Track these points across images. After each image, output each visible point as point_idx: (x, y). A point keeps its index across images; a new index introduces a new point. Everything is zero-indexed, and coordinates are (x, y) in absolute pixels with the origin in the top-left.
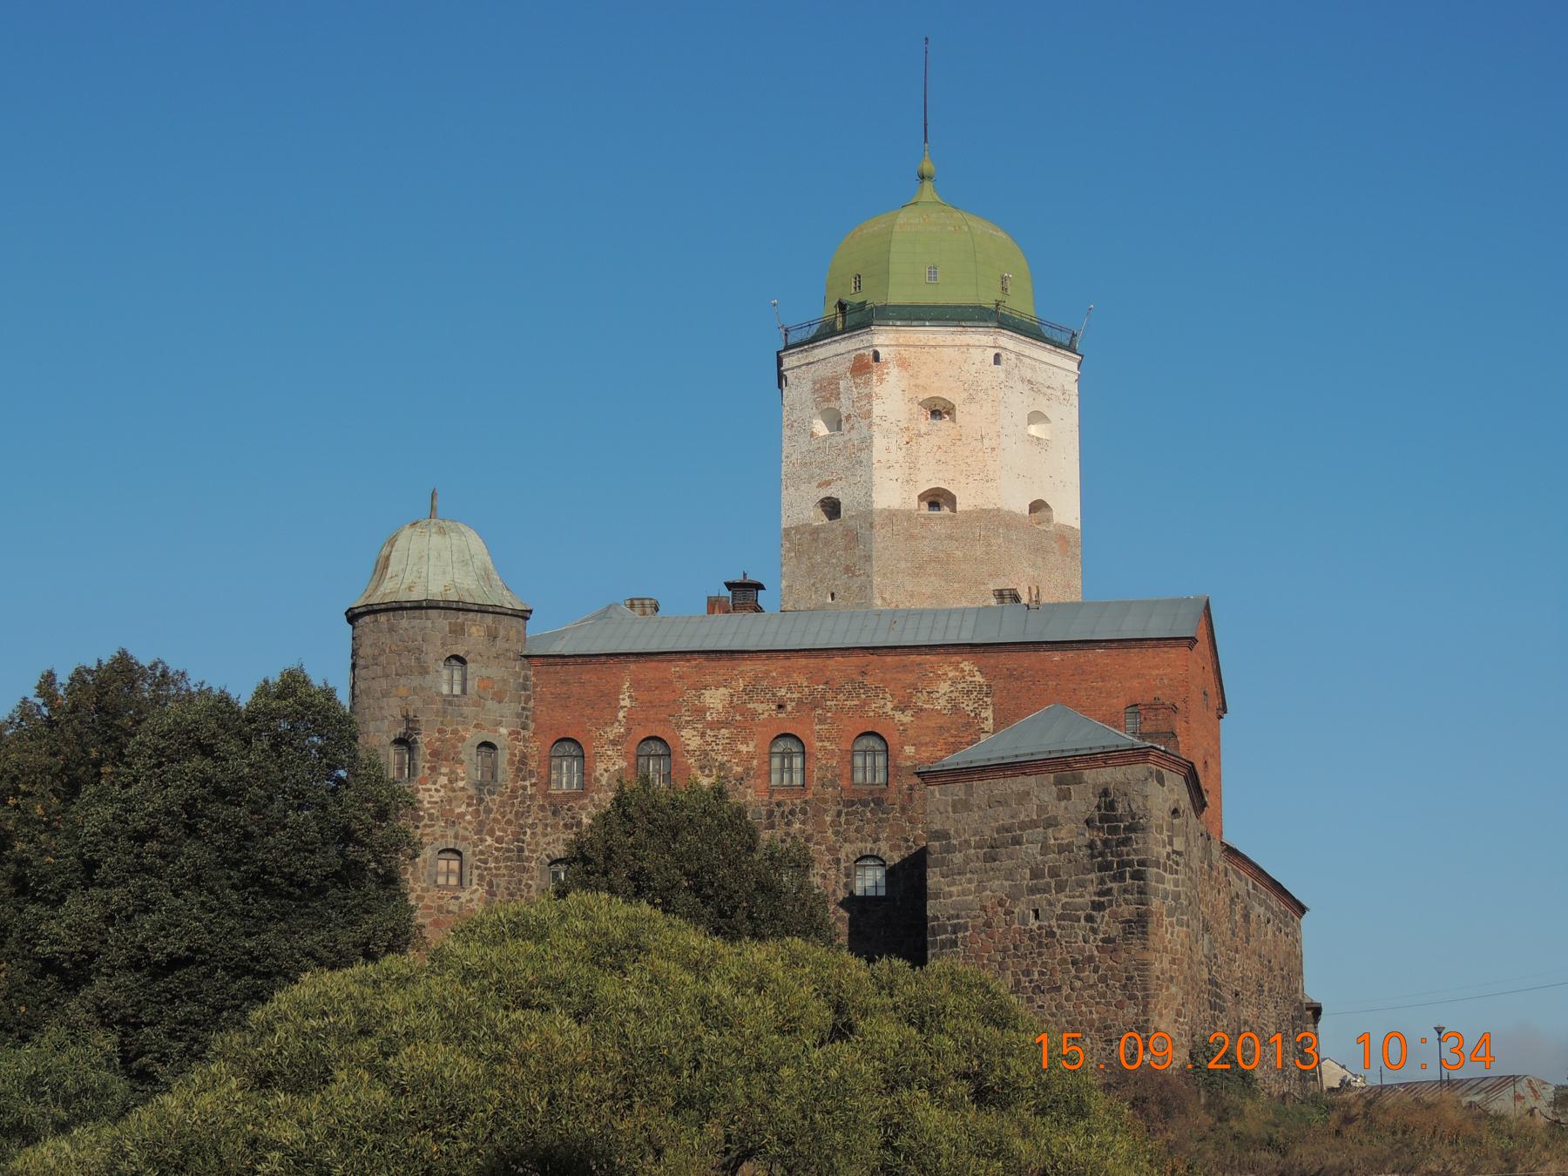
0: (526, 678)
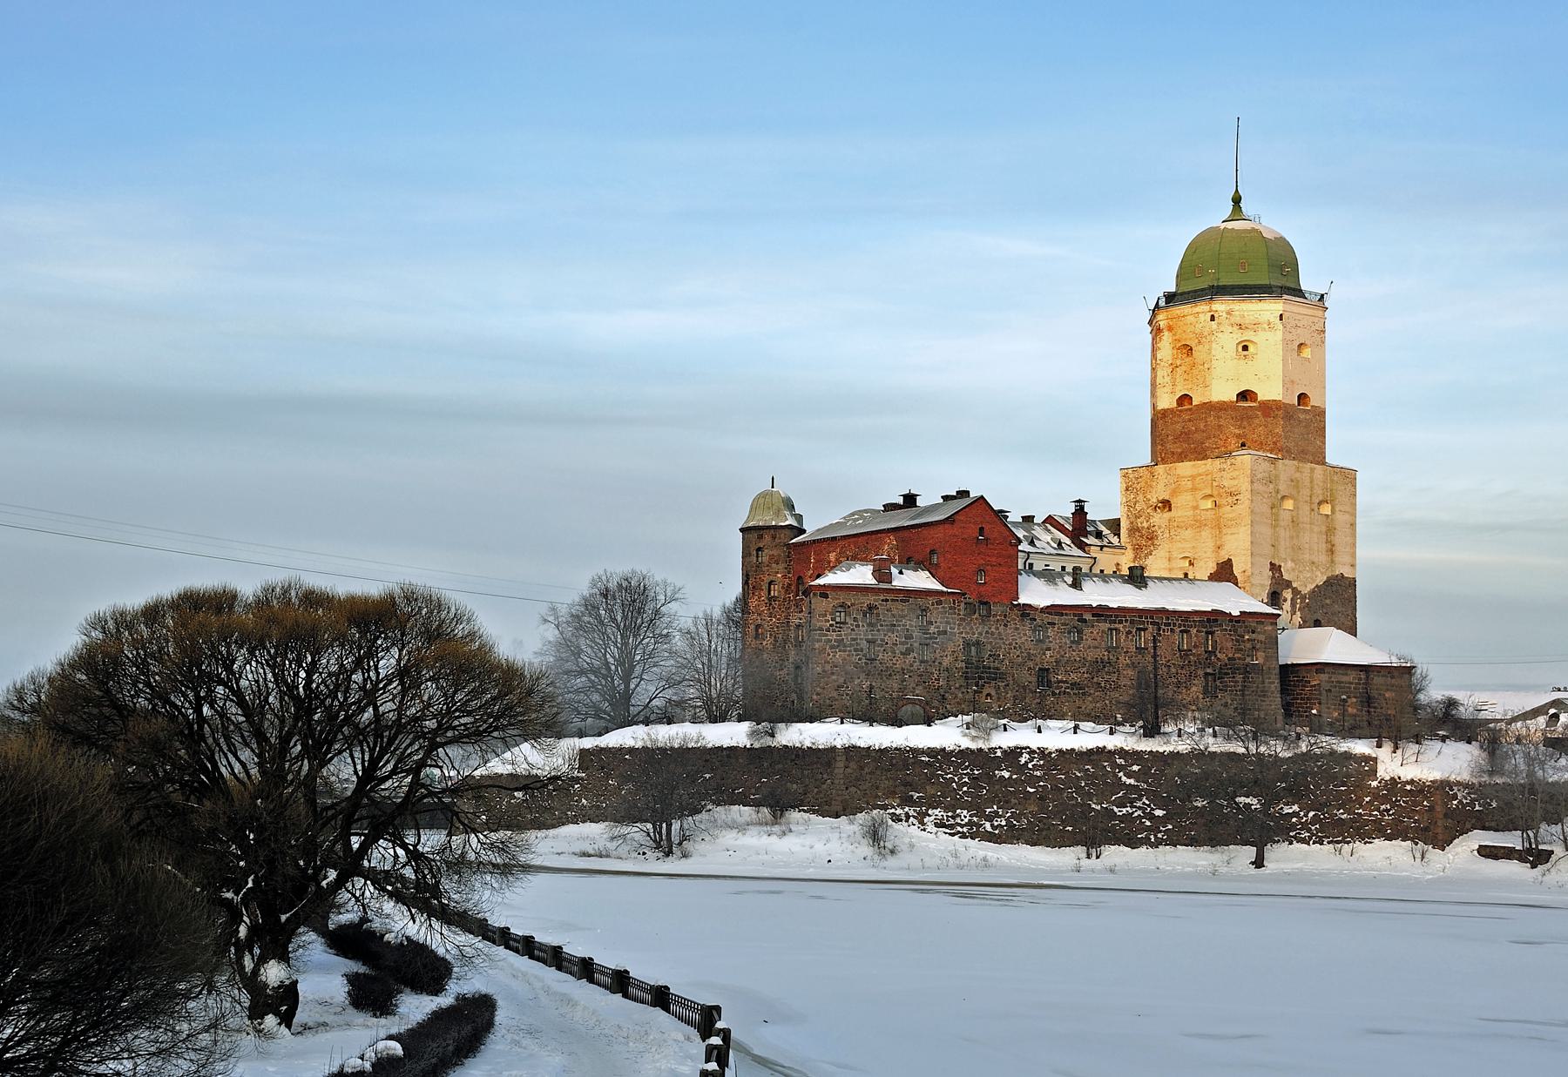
0: (789, 553)
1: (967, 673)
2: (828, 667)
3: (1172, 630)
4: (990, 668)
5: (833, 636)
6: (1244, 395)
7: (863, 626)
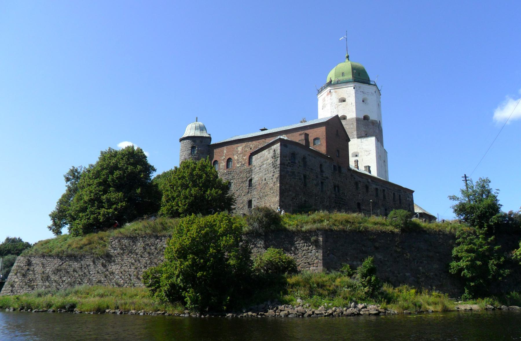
1: (335, 200)
2: (287, 187)
3: (391, 192)
4: (343, 199)
5: (289, 169)
6: (366, 118)
7: (302, 167)
